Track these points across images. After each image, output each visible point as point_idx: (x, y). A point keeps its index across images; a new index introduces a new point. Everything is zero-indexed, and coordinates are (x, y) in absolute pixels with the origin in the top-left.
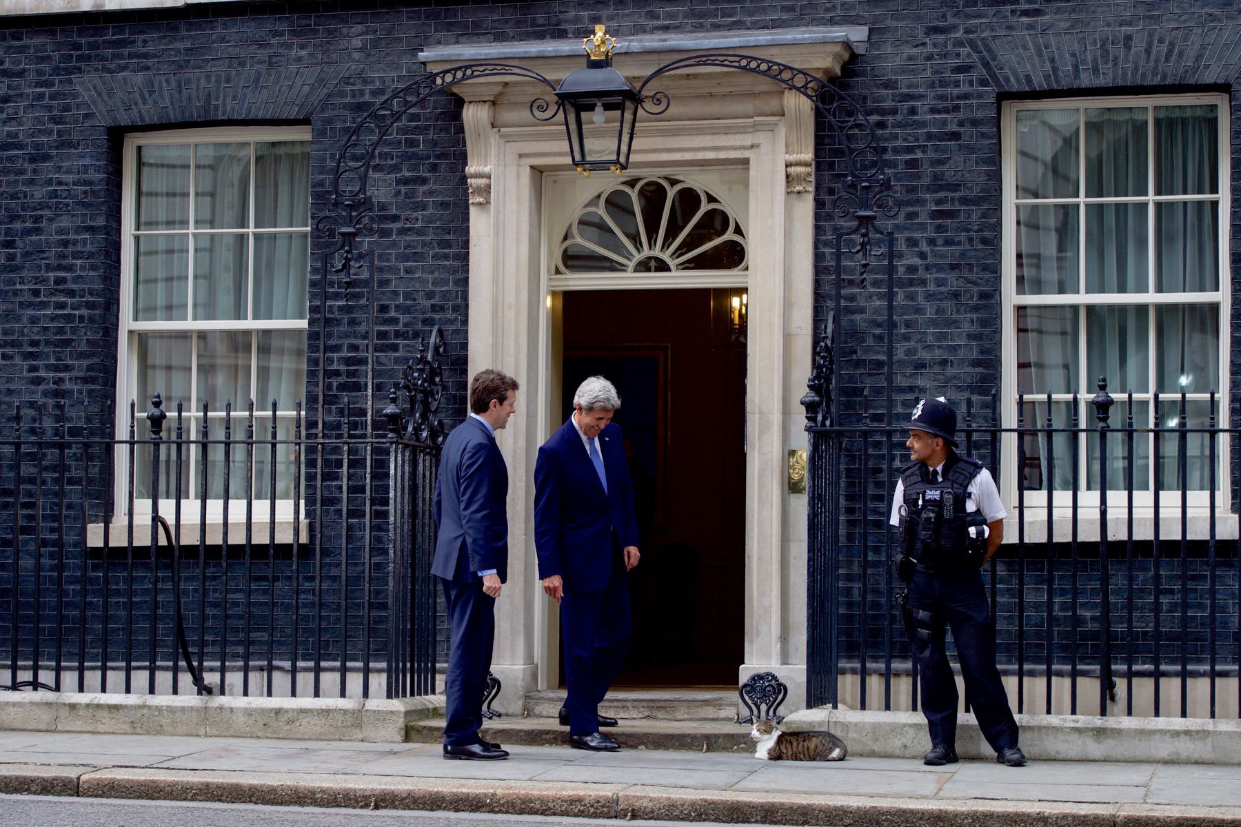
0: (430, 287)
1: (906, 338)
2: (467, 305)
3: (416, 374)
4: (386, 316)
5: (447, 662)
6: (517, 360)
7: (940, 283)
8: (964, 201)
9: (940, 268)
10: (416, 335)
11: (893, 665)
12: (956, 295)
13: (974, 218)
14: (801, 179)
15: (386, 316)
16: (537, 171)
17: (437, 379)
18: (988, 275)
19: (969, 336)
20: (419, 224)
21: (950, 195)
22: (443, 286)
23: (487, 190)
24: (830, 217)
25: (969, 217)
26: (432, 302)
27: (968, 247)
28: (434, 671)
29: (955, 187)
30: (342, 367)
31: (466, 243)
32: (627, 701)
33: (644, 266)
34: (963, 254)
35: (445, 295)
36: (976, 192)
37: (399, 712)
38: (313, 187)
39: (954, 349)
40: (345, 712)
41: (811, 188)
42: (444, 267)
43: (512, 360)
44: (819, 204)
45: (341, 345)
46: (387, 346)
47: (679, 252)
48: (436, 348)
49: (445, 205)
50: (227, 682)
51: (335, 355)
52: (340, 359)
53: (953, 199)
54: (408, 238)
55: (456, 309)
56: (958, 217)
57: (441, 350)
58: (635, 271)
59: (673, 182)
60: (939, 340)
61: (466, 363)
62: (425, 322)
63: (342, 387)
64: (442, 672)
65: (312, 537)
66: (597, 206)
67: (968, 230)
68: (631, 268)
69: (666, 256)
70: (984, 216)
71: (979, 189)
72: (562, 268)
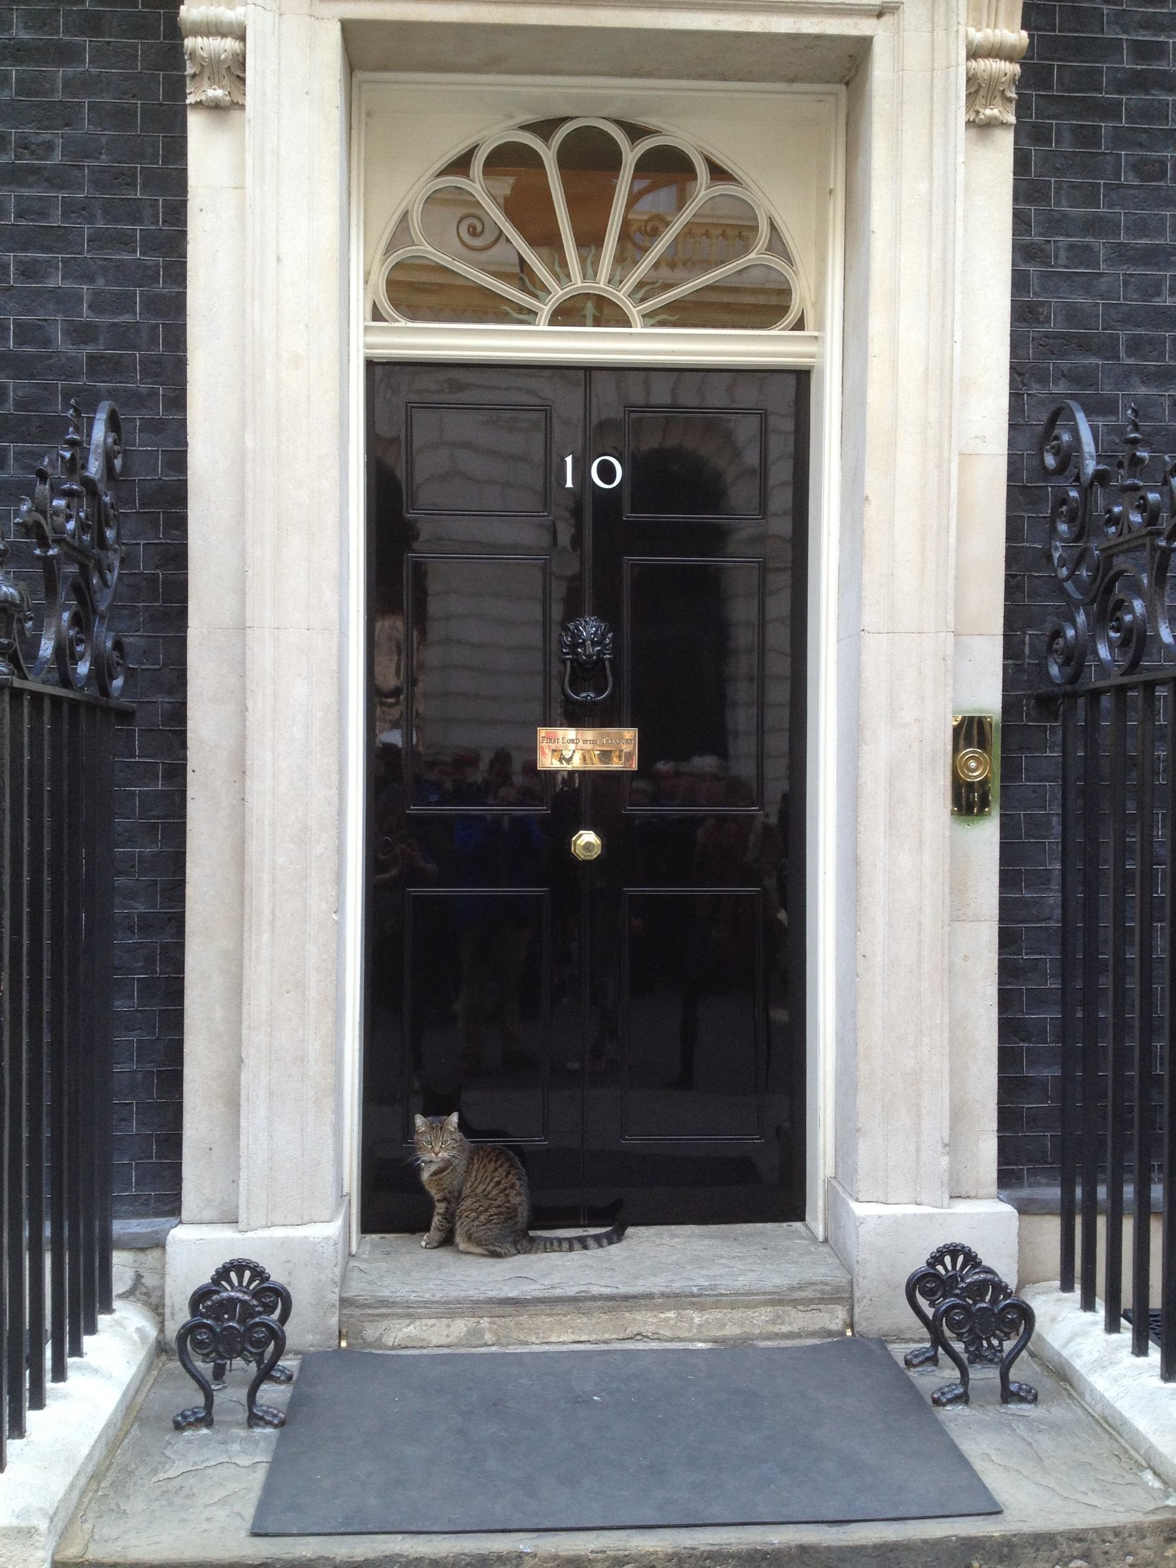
0: (86, 315)
3: (59, 503)
17: (110, 534)
20: (57, 158)
23: (235, 70)
26: (90, 349)
33: (566, 314)
41: (1012, 119)
44: (1021, 163)
47: (644, 289)
48: (109, 458)
49: (122, 117)
54: (26, 192)
57: (118, 463)
58: (552, 323)
59: (636, 132)
66: (467, 176)
69: (621, 296)
72: (386, 307)
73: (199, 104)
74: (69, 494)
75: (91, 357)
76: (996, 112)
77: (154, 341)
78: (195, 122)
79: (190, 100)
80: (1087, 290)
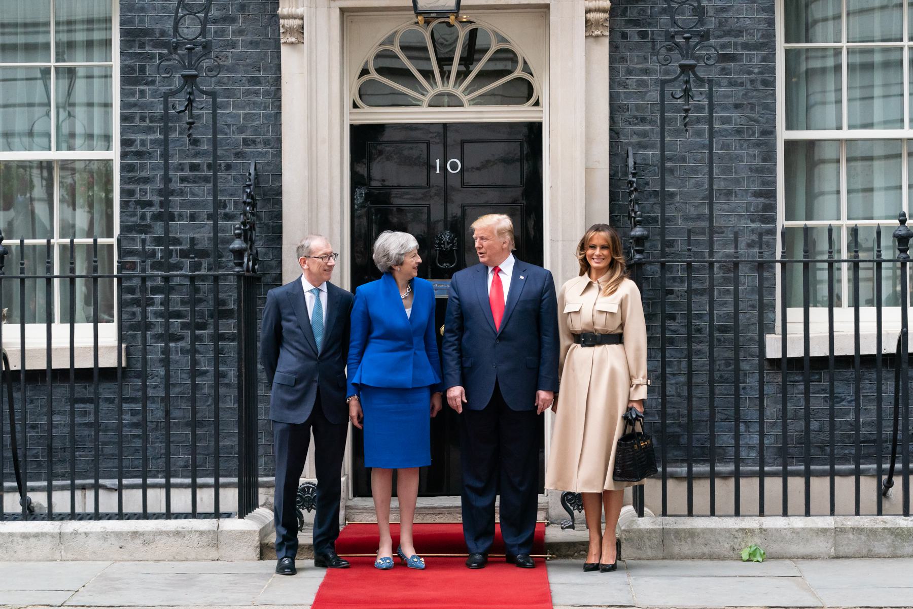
1: (695, 171)
2: (279, 140)
4: (199, 149)
5: (273, 476)
6: (331, 191)
7: (726, 120)
8: (745, 46)
9: (725, 108)
10: (229, 167)
11: (694, 469)
12: (739, 132)
13: (756, 61)
14: (598, 24)
15: (199, 149)
16: (342, 10)
18: (768, 114)
19: (751, 170)
20: (230, 62)
21: (733, 39)
22: (254, 121)
24: (623, 59)
25: (750, 61)
26: (243, 136)
27: (749, 88)
28: (257, 485)
29: (739, 33)
30: (156, 199)
31: (278, 80)
32: (444, 508)
34: (745, 94)
35: (256, 130)
36: (758, 38)
37: (255, 531)
38: (121, 24)
39: (737, 181)
40: (201, 533)
41: (608, 34)
42: (255, 103)
43: (327, 192)
44: (613, 47)
45: (154, 177)
46: (200, 178)
47: (469, 90)
49: (254, 44)
50: (54, 500)
51: (148, 187)
52: (153, 190)
53: (736, 44)
55: (266, 143)
56: (741, 60)
58: (430, 106)
60: (724, 172)
61: (280, 194)
62: (238, 155)
63: (156, 217)
64: (267, 485)
65: (128, 360)
67: (750, 73)
68: (425, 104)
69: (459, 91)
70: (764, 59)
71: (759, 35)
72: (359, 102)
73: (285, 43)
74: (249, 204)
75: (244, 139)
76: (599, 33)
77: (268, 131)
78: (284, 49)
79: (282, 41)
80: (643, 99)
